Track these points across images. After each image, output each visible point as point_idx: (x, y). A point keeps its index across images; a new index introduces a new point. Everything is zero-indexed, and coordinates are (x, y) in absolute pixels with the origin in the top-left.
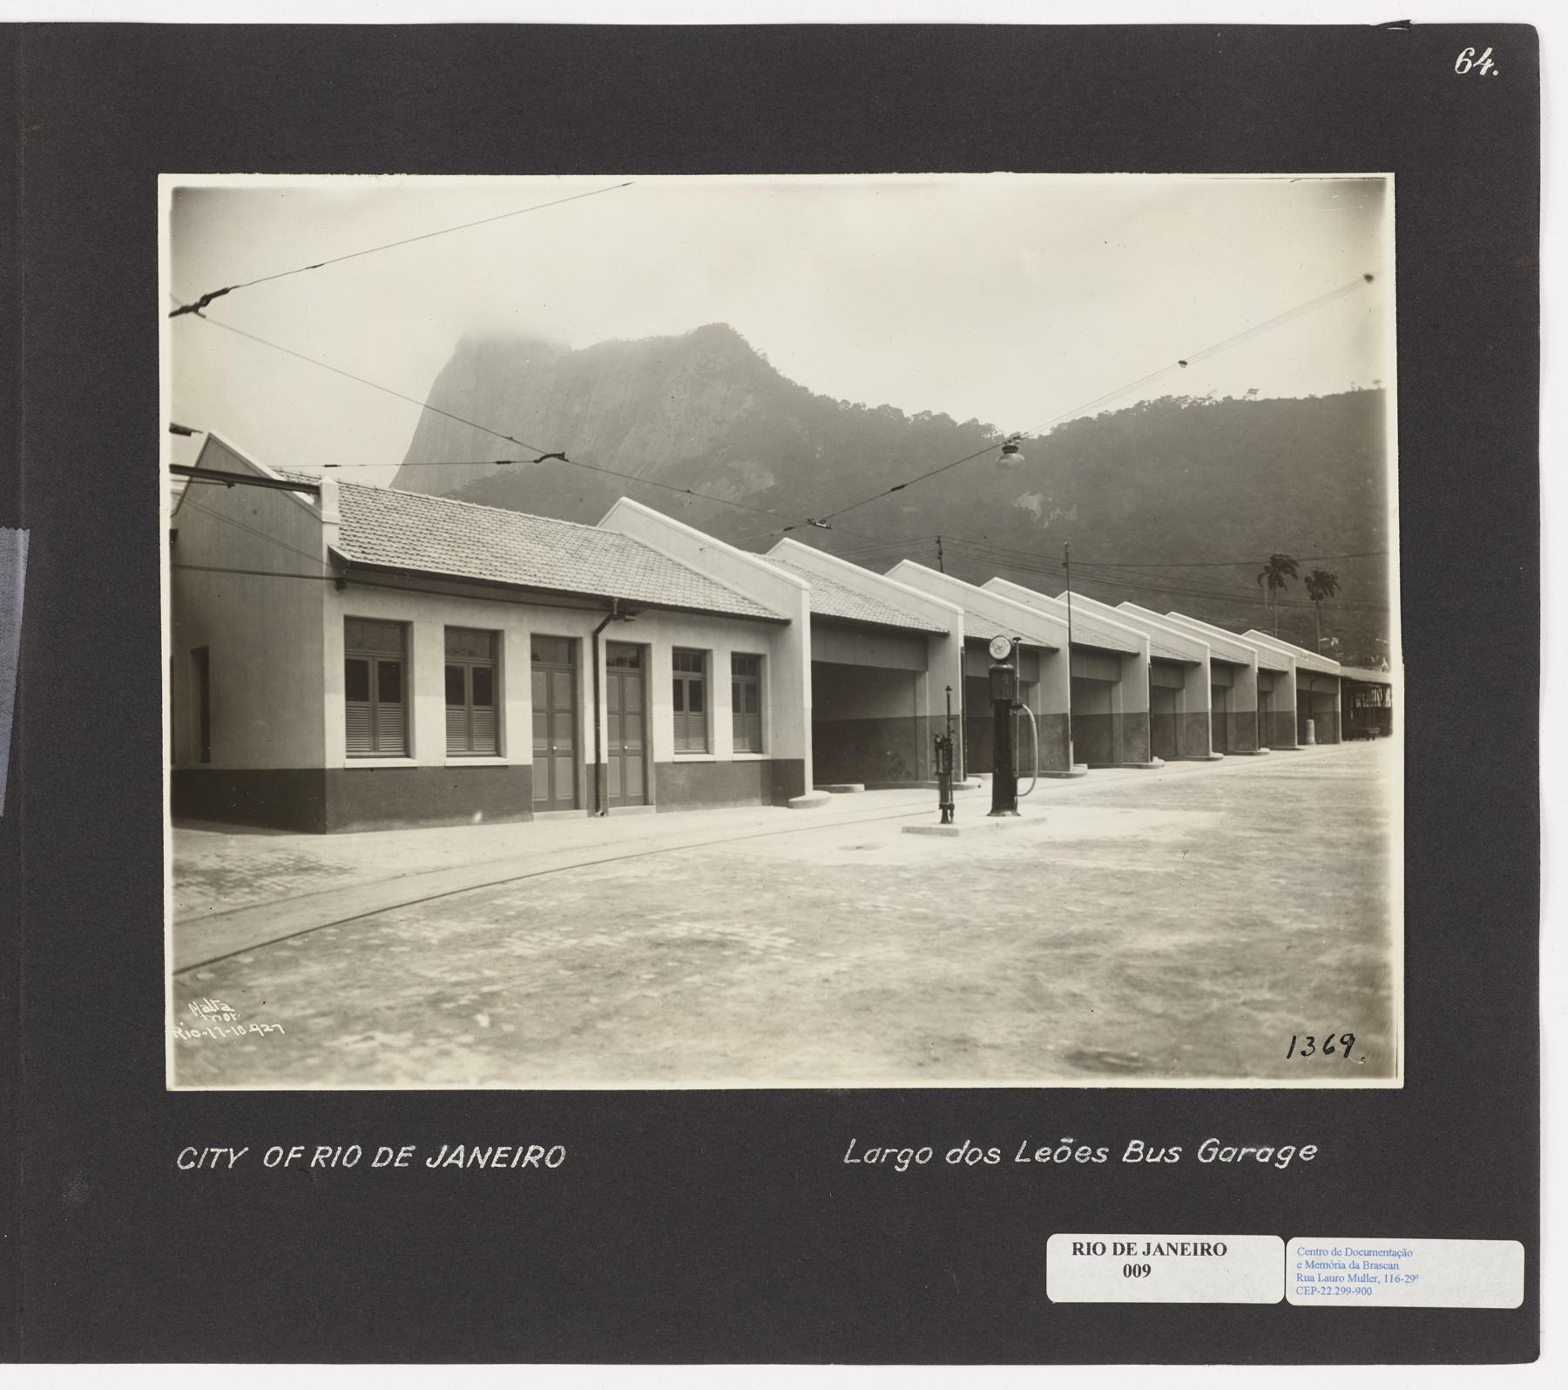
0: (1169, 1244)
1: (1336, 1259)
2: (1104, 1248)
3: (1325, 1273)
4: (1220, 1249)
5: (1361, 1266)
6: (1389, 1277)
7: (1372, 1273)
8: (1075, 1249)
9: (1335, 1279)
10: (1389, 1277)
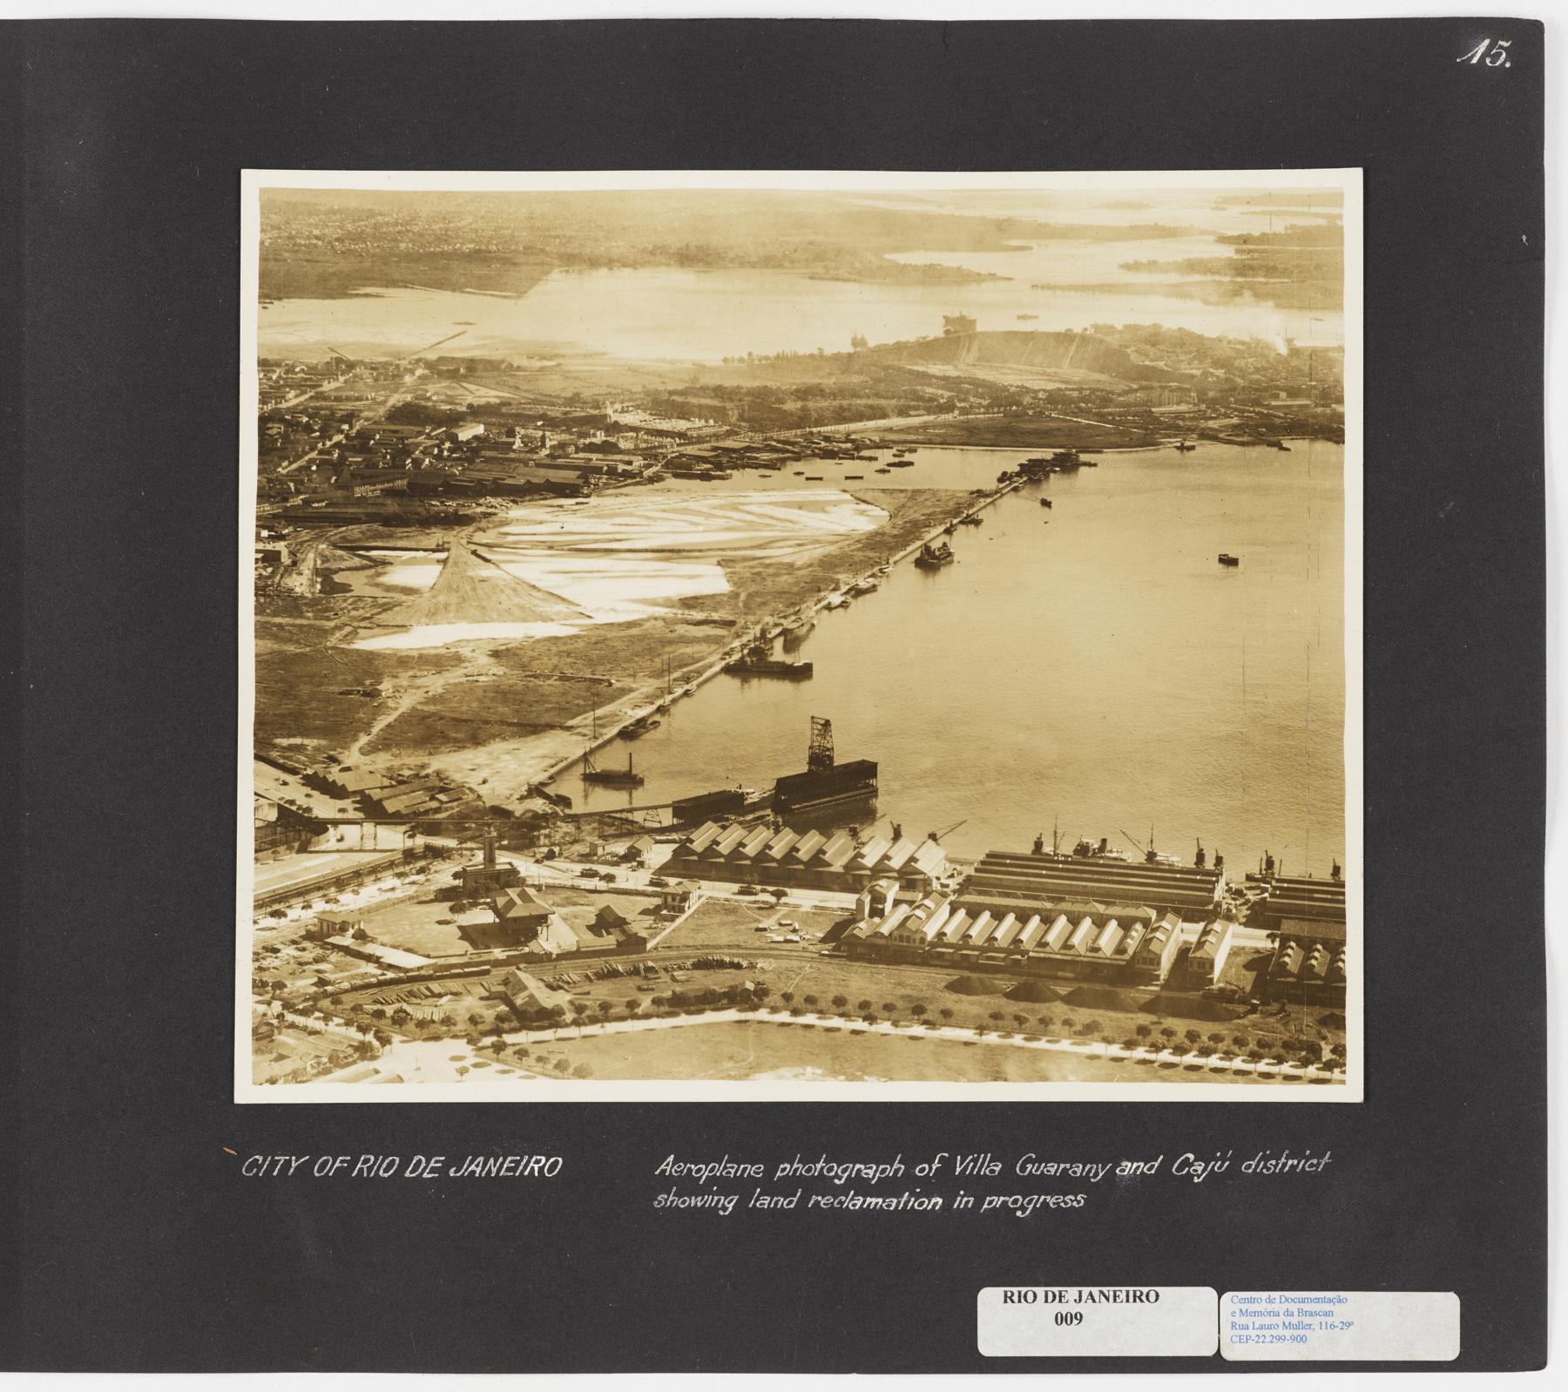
0: (1101, 1292)
1: (1270, 1307)
2: (1035, 1296)
3: (1259, 1321)
4: (1152, 1296)
5: (1296, 1313)
6: (1324, 1324)
7: (1307, 1320)
8: (1006, 1296)
9: (1270, 1327)
10: (1324, 1324)
